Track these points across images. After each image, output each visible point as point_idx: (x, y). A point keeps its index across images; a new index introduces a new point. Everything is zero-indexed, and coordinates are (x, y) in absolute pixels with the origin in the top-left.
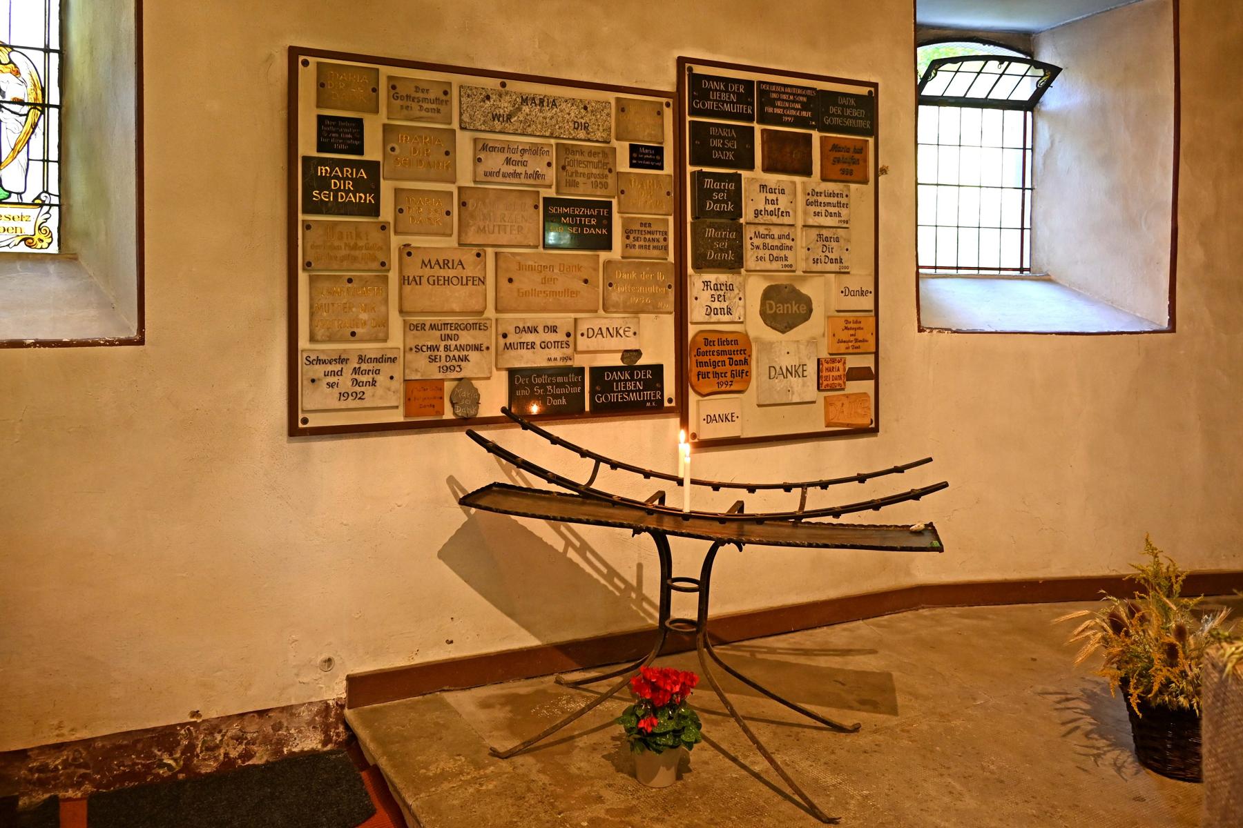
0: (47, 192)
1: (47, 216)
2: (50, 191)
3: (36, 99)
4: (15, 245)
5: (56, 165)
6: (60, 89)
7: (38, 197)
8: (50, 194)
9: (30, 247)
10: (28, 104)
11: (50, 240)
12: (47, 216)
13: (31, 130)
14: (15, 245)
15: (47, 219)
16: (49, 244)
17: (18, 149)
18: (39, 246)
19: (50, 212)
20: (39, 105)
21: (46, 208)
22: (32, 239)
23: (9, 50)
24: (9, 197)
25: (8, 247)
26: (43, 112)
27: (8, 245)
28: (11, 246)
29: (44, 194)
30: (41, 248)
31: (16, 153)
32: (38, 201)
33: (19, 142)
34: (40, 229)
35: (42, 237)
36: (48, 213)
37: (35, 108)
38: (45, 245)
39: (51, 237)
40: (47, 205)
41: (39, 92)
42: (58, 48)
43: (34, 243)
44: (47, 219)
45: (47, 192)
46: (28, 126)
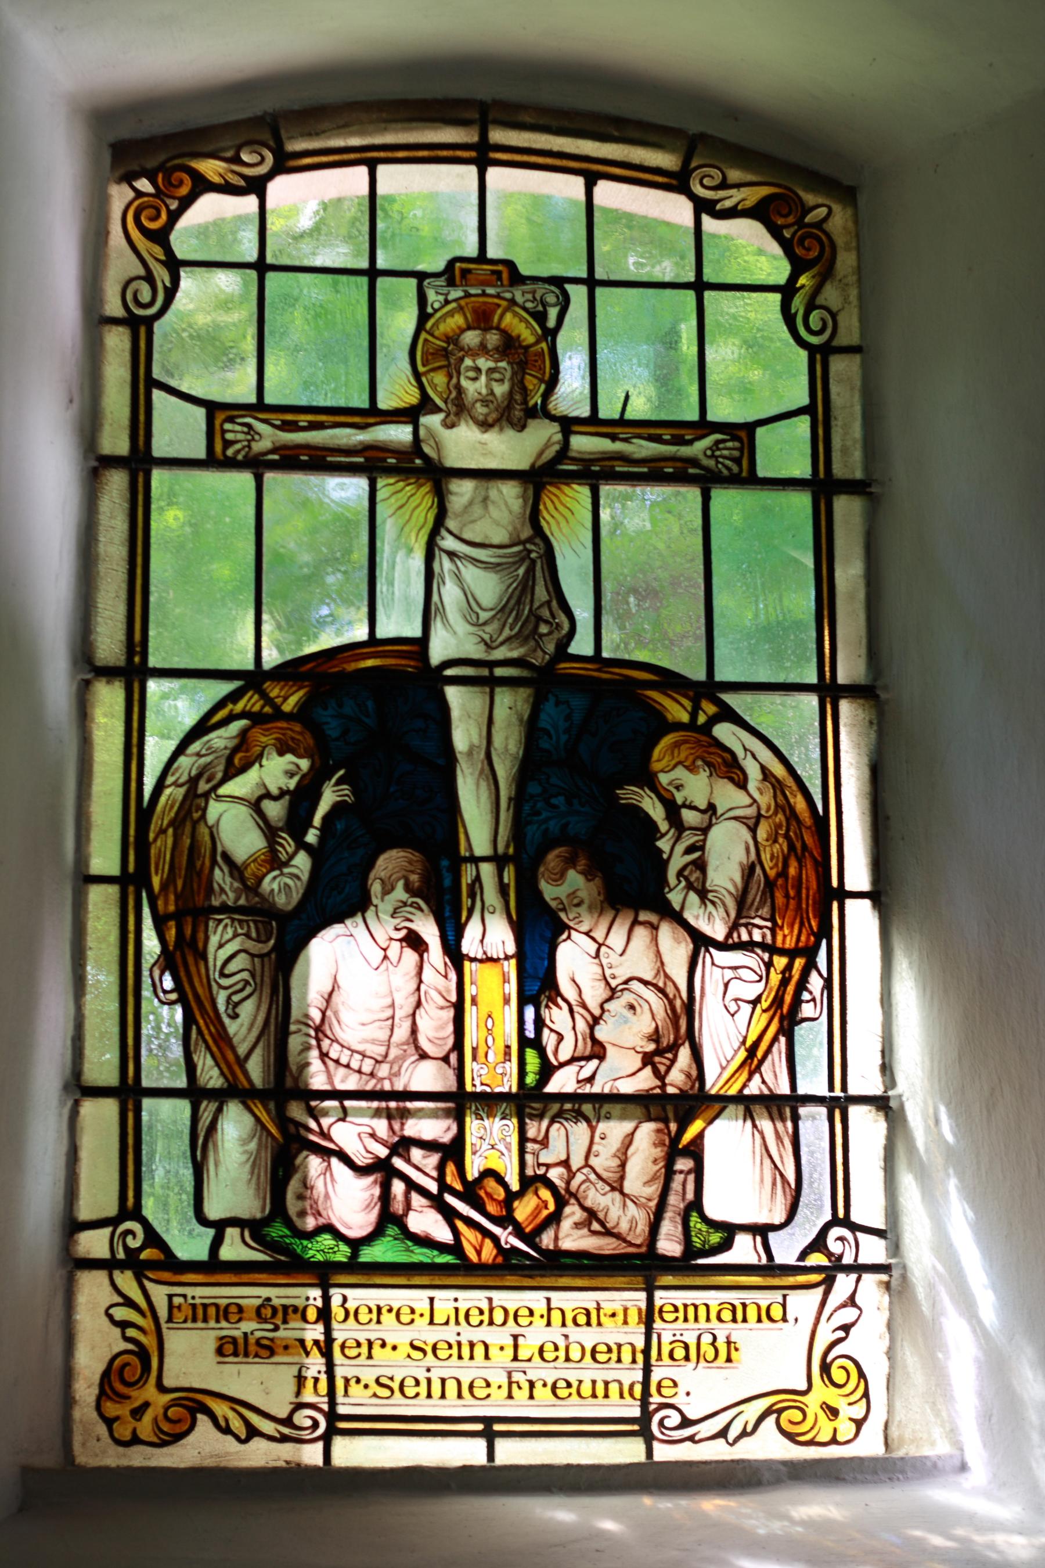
0: (847, 1222)
1: (848, 1315)
2: (855, 1217)
4: (744, 1434)
8: (854, 1228)
9: (791, 1437)
11: (859, 1411)
12: (848, 1315)
14: (744, 1434)
15: (846, 1328)
16: (859, 1423)
19: (858, 1300)
27: (723, 1433)
28: (732, 1434)
29: (836, 1232)
30: (834, 1441)
32: (817, 1259)
34: (826, 1368)
36: (851, 1301)
38: (846, 1429)
40: (848, 1269)
44: (846, 1328)
45: (847, 1222)
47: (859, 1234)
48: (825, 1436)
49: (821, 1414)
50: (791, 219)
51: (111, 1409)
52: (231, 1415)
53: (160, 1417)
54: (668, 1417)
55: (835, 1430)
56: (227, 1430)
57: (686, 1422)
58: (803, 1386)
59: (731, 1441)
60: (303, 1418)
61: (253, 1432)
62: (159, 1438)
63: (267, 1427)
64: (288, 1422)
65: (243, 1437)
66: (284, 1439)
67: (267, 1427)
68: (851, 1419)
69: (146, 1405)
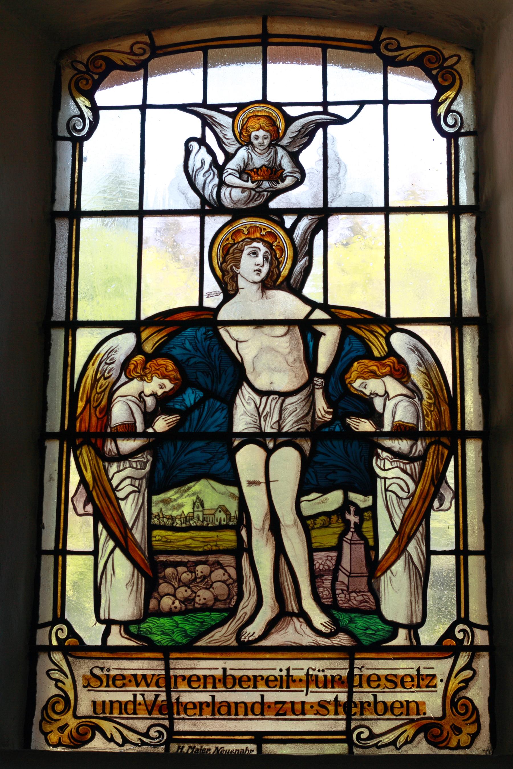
1: (468, 674)
3: (439, 424)
4: (406, 742)
5: (481, 559)
6: (483, 398)
7: (450, 633)
8: (472, 625)
10: (424, 435)
11: (472, 729)
12: (468, 674)
13: (433, 489)
14: (406, 742)
15: (467, 682)
16: (474, 737)
17: (407, 530)
18: (454, 743)
19: (474, 665)
20: (445, 434)
21: (463, 660)
22: (440, 727)
23: (388, 329)
24: (394, 635)
25: (392, 747)
26: (453, 451)
27: (393, 743)
29: (461, 626)
30: (458, 747)
31: (405, 539)
32: (449, 642)
33: (411, 515)
34: (454, 704)
35: (459, 721)
36: (468, 666)
37: (438, 443)
38: (464, 739)
39: (477, 721)
40: (466, 649)
41: (444, 408)
42: (475, 313)
43: (445, 734)
44: (467, 682)
46: (425, 482)
49: (451, 731)
50: (437, 65)
52: (114, 731)
54: (363, 732)
55: (459, 740)
56: (111, 740)
57: (372, 736)
58: (440, 714)
61: (125, 741)
63: (133, 737)
64: (146, 735)
66: (143, 743)
67: (133, 737)
68: (468, 734)
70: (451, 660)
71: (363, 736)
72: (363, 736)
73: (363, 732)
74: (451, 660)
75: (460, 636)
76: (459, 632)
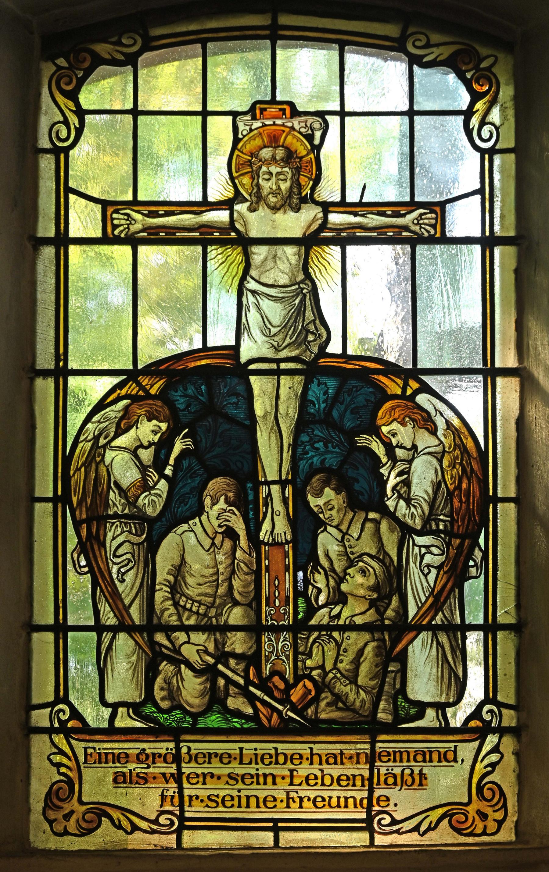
0: (494, 701)
1: (494, 757)
4: (429, 829)
8: (500, 705)
11: (499, 816)
12: (494, 757)
14: (429, 829)
16: (500, 823)
19: (501, 749)
21: (491, 740)
27: (416, 829)
32: (473, 724)
34: (480, 789)
36: (495, 749)
38: (492, 826)
39: (505, 806)
40: (494, 731)
44: (493, 765)
47: (502, 709)
48: (478, 831)
49: (477, 818)
51: (52, 815)
52: (122, 818)
53: (81, 819)
56: (119, 827)
57: (394, 822)
58: (465, 800)
59: (421, 833)
60: (163, 820)
61: (135, 828)
62: (80, 831)
63: (143, 825)
64: (156, 822)
65: (129, 831)
66: (153, 832)
67: (143, 825)
69: (72, 812)
70: (476, 744)
71: (384, 822)
72: (384, 822)
73: (384, 819)
74: (476, 744)
75: (487, 717)
76: (487, 712)
